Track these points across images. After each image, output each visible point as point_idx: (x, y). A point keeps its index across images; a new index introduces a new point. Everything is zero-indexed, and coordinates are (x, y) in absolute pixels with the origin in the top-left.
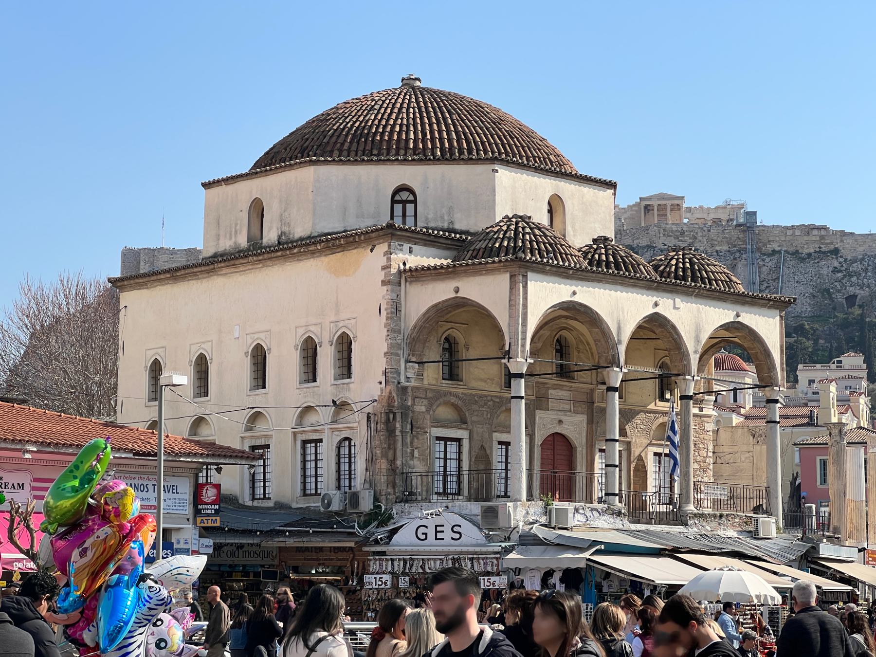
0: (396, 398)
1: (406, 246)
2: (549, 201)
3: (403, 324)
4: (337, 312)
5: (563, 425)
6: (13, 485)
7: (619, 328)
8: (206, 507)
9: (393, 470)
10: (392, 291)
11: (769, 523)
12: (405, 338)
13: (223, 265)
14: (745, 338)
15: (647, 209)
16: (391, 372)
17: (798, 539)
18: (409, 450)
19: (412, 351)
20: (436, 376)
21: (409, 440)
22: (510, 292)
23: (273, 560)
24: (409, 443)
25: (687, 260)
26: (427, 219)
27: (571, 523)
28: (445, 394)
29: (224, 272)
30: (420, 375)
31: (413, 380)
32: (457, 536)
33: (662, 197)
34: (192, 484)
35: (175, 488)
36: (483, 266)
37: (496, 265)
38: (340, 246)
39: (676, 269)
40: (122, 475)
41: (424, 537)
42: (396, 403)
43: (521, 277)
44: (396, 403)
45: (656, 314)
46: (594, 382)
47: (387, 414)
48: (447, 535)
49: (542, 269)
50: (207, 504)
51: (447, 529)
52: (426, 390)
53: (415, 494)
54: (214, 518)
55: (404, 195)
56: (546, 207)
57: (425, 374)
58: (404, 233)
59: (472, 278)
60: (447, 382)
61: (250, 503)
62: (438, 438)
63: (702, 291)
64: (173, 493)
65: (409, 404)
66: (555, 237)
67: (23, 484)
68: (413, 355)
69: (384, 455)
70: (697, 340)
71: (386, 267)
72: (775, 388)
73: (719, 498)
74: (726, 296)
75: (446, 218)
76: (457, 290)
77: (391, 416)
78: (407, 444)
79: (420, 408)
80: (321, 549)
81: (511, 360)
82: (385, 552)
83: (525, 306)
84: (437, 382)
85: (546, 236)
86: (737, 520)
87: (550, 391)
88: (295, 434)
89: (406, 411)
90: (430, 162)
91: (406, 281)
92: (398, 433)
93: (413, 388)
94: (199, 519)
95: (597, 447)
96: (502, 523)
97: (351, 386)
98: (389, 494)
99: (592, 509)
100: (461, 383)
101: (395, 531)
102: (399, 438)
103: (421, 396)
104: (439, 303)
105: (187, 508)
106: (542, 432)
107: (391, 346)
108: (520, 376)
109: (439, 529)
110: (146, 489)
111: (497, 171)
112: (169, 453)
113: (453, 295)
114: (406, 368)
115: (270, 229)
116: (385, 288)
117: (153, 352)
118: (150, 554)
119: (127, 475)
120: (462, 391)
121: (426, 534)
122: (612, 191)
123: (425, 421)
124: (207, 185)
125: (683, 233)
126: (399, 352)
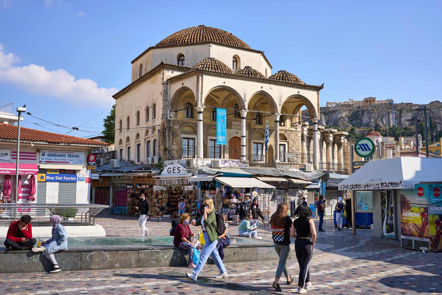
0: (165, 124)
1: (170, 71)
2: (233, 57)
3: (169, 98)
4: (153, 97)
5: (238, 134)
6: (3, 154)
7: (245, 96)
8: (91, 162)
9: (165, 149)
10: (164, 87)
11: (310, 166)
12: (170, 103)
13: (131, 86)
14: (303, 101)
15: (367, 101)
16: (164, 115)
17: (322, 172)
18: (171, 142)
19: (172, 107)
20: (183, 116)
21: (171, 138)
22: (197, 82)
23: (132, 182)
24: (171, 140)
25: (282, 74)
26: (188, 64)
27: (221, 165)
28: (187, 123)
29: (133, 88)
30: (176, 116)
31: (173, 118)
32: (179, 171)
33: (370, 98)
34: (86, 155)
35: (78, 156)
36: (189, 74)
37: (192, 73)
38: (153, 74)
39: (277, 78)
40: (53, 151)
41: (169, 172)
42: (166, 126)
43: (200, 76)
44: (166, 126)
45: (262, 91)
46: (251, 119)
47: (163, 129)
48: (176, 171)
49: (209, 73)
50: (91, 161)
51: (176, 169)
52: (179, 121)
53: (173, 157)
54: (93, 166)
55: (182, 58)
56: (232, 59)
57: (178, 116)
58: (168, 66)
59: (187, 79)
60: (188, 118)
61: (137, 164)
62: (184, 138)
63: (282, 83)
64: (77, 157)
65: (172, 126)
66: (220, 64)
67: (7, 154)
68: (173, 109)
69: (163, 144)
70: (280, 101)
71: (163, 79)
72: (315, 119)
73: (292, 158)
74: (293, 85)
75: (194, 64)
76: (183, 84)
77: (164, 130)
78: (170, 140)
79: (176, 127)
80: (143, 177)
81: (197, 107)
82: (159, 178)
83: (202, 87)
84: (183, 118)
85: (216, 63)
86: (298, 165)
87: (233, 122)
88: (145, 139)
89: (170, 129)
90: (189, 45)
91: (170, 83)
92: (167, 136)
93: (173, 120)
94: (89, 167)
95: (252, 141)
96: (191, 166)
97: (155, 121)
98: (164, 158)
99: (233, 161)
100: (194, 119)
101: (162, 170)
102: (167, 138)
103: (177, 123)
104: (179, 89)
105: (84, 163)
106: (229, 136)
107: (164, 106)
108: (200, 112)
109: (174, 169)
110: (64, 156)
111: (211, 46)
112: (68, 143)
113: (182, 86)
114: (170, 113)
115: (143, 73)
116: (162, 86)
117: (120, 117)
118: (66, 179)
119: (55, 151)
120: (194, 122)
121: (170, 171)
122: (261, 54)
123: (178, 132)
124: (132, 62)
125: (375, 106)
126: (167, 108)
